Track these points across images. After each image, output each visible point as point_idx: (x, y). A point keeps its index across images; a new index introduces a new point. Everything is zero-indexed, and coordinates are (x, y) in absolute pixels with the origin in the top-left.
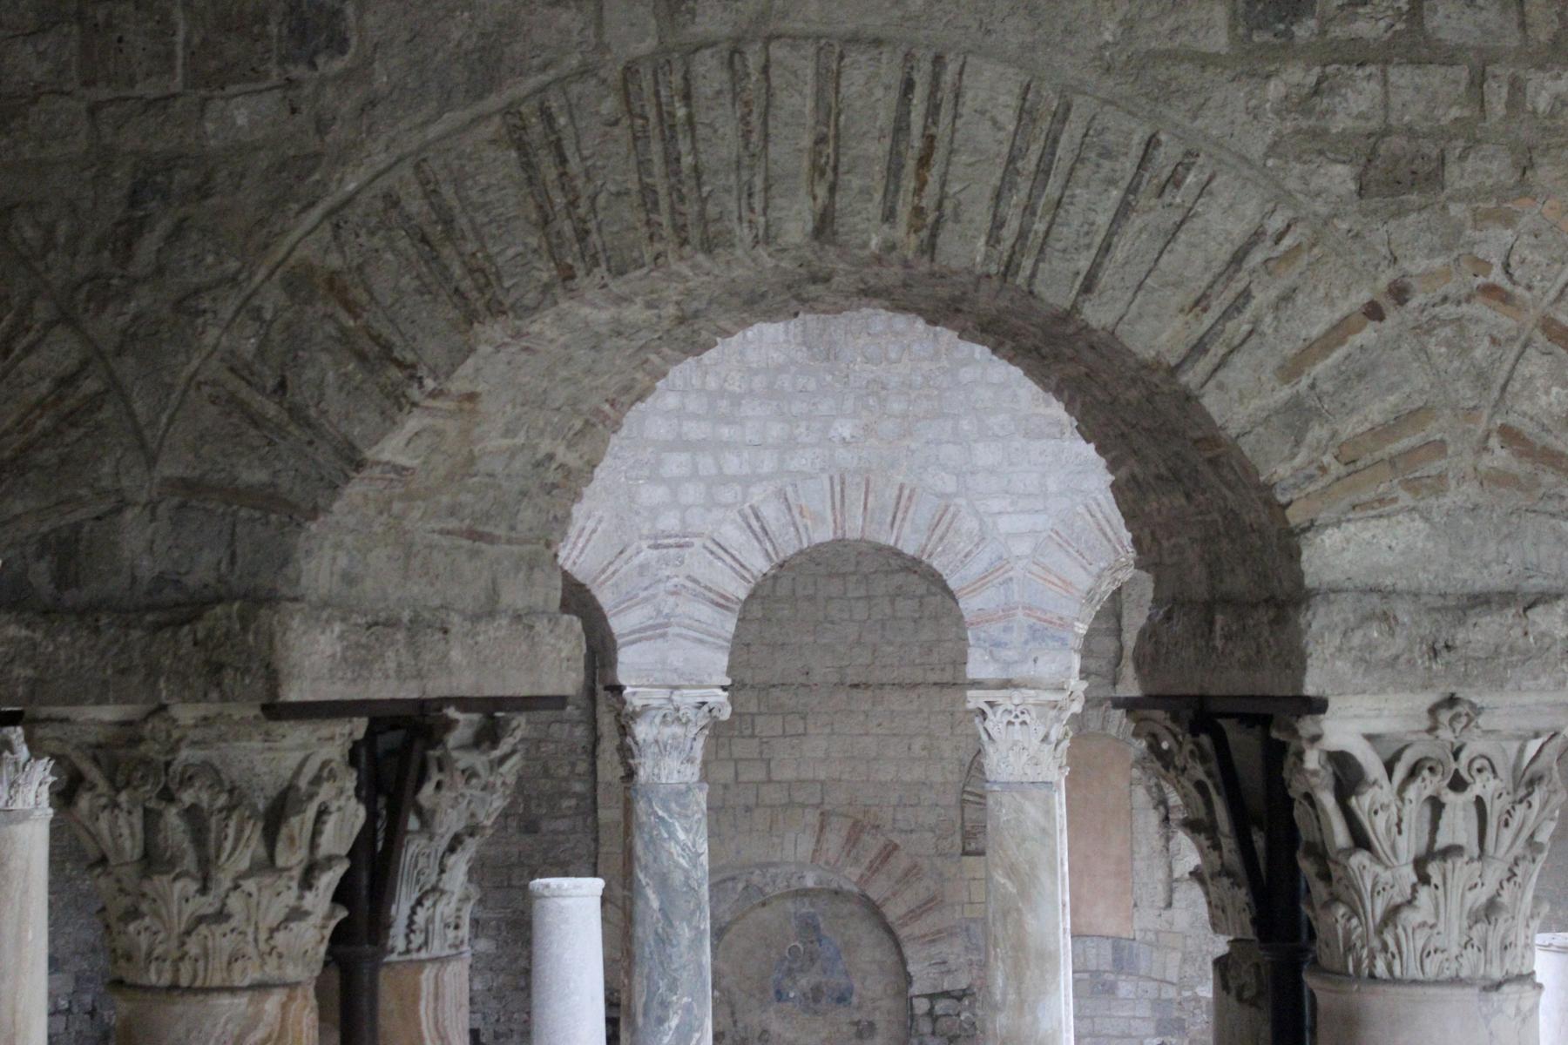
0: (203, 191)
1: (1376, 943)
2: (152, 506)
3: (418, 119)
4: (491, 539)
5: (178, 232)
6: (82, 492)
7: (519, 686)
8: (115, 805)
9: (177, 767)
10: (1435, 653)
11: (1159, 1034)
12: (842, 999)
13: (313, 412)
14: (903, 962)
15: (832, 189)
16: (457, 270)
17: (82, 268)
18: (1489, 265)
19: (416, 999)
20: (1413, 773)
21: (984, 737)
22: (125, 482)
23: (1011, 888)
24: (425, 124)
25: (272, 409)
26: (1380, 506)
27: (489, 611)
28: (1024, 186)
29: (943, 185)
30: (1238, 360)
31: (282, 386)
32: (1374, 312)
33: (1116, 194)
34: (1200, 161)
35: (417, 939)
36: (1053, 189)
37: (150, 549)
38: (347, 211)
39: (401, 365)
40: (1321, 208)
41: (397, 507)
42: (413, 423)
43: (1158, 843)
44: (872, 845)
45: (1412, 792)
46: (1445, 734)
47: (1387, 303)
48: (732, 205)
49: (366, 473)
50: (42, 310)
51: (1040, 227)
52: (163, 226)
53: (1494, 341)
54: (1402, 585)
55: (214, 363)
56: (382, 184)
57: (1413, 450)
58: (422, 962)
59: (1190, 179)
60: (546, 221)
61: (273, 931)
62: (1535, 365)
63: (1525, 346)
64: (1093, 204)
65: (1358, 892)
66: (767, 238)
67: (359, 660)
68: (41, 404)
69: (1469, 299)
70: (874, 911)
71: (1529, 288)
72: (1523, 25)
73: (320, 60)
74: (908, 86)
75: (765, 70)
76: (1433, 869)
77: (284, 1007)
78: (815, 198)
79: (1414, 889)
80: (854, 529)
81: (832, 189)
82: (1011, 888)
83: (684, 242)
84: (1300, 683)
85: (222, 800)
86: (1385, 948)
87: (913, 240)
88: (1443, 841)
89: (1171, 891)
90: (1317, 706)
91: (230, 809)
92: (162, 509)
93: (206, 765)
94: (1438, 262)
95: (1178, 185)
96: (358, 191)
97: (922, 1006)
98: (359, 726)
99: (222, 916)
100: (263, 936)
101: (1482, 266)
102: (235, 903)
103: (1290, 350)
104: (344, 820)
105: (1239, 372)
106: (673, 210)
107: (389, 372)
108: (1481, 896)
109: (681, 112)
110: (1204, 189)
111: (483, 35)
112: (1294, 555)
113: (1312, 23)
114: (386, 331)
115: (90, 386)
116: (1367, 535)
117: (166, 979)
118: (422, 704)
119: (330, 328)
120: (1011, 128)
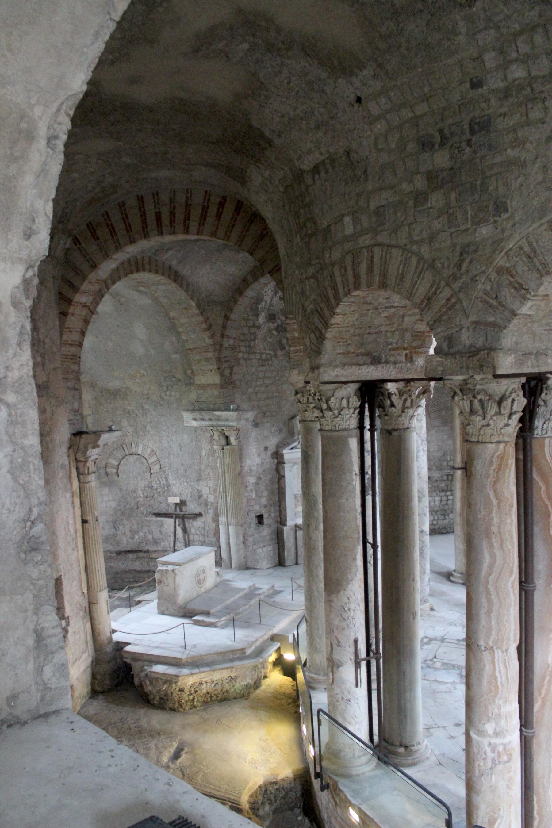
0: (476, 251)
2: (468, 328)
3: (526, 227)
5: (471, 262)
9: (476, 390)
13: (504, 303)
17: (451, 272)
19: (544, 446)
22: (462, 323)
24: (528, 228)
25: (494, 303)
31: (497, 297)
35: (544, 432)
37: (468, 339)
38: (510, 252)
39: (525, 289)
41: (529, 325)
42: (529, 304)
49: (517, 317)
52: (467, 261)
55: (481, 292)
56: (519, 244)
58: (545, 437)
61: (501, 429)
67: (520, 363)
68: (443, 306)
73: (502, 215)
77: (505, 447)
85: (487, 398)
91: (489, 400)
92: (471, 329)
93: (484, 390)
98: (523, 380)
99: (488, 425)
100: (499, 430)
102: (491, 422)
104: (521, 402)
107: (522, 291)
111: (542, 203)
114: (521, 281)
115: (454, 300)
117: (476, 440)
118: (540, 374)
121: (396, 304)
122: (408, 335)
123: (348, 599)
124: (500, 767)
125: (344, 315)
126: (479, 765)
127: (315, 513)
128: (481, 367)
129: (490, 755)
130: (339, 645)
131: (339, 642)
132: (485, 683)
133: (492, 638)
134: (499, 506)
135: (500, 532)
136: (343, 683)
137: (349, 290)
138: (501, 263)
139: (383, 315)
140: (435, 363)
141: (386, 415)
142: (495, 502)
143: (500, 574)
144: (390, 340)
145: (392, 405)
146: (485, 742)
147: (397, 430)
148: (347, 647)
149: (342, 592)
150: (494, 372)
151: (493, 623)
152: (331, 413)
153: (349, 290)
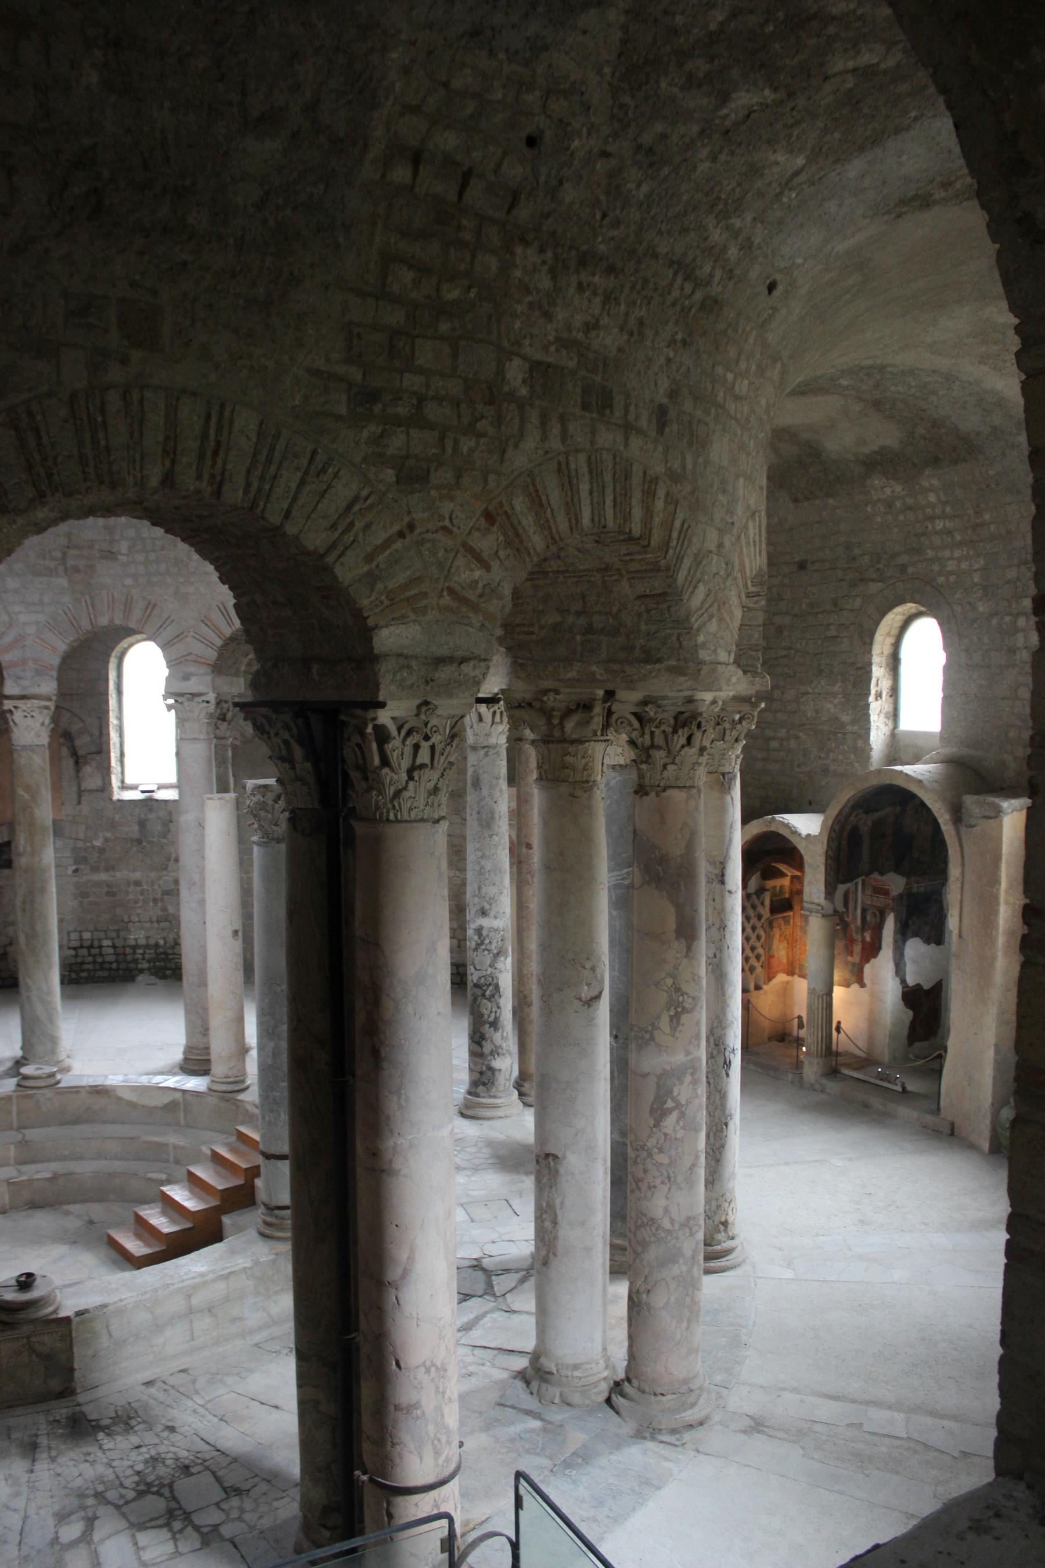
1: (390, 806)
10: (427, 682)
11: (75, 864)
15: (173, 462)
18: (444, 518)
21: (11, 723)
23: (27, 797)
26: (402, 619)
29: (225, 464)
30: (349, 553)
32: (401, 535)
33: (299, 474)
34: (335, 463)
36: (273, 469)
40: (383, 489)
43: (73, 773)
45: (408, 742)
46: (423, 717)
51: (267, 487)
53: (446, 550)
54: (410, 653)
57: (416, 595)
59: (330, 470)
62: (460, 561)
63: (457, 553)
65: (383, 785)
69: (436, 531)
71: (459, 528)
72: (459, 417)
74: (208, 417)
75: (141, 402)
76: (416, 774)
78: (164, 465)
79: (407, 783)
81: (173, 462)
82: (27, 797)
83: (102, 483)
84: (378, 697)
86: (394, 807)
87: (209, 489)
88: (419, 761)
89: (80, 796)
90: (382, 705)
94: (426, 515)
95: (325, 473)
101: (442, 518)
103: (369, 549)
108: (432, 784)
109: (100, 419)
110: (336, 475)
113: (380, 406)
116: (398, 631)
120: (255, 440)
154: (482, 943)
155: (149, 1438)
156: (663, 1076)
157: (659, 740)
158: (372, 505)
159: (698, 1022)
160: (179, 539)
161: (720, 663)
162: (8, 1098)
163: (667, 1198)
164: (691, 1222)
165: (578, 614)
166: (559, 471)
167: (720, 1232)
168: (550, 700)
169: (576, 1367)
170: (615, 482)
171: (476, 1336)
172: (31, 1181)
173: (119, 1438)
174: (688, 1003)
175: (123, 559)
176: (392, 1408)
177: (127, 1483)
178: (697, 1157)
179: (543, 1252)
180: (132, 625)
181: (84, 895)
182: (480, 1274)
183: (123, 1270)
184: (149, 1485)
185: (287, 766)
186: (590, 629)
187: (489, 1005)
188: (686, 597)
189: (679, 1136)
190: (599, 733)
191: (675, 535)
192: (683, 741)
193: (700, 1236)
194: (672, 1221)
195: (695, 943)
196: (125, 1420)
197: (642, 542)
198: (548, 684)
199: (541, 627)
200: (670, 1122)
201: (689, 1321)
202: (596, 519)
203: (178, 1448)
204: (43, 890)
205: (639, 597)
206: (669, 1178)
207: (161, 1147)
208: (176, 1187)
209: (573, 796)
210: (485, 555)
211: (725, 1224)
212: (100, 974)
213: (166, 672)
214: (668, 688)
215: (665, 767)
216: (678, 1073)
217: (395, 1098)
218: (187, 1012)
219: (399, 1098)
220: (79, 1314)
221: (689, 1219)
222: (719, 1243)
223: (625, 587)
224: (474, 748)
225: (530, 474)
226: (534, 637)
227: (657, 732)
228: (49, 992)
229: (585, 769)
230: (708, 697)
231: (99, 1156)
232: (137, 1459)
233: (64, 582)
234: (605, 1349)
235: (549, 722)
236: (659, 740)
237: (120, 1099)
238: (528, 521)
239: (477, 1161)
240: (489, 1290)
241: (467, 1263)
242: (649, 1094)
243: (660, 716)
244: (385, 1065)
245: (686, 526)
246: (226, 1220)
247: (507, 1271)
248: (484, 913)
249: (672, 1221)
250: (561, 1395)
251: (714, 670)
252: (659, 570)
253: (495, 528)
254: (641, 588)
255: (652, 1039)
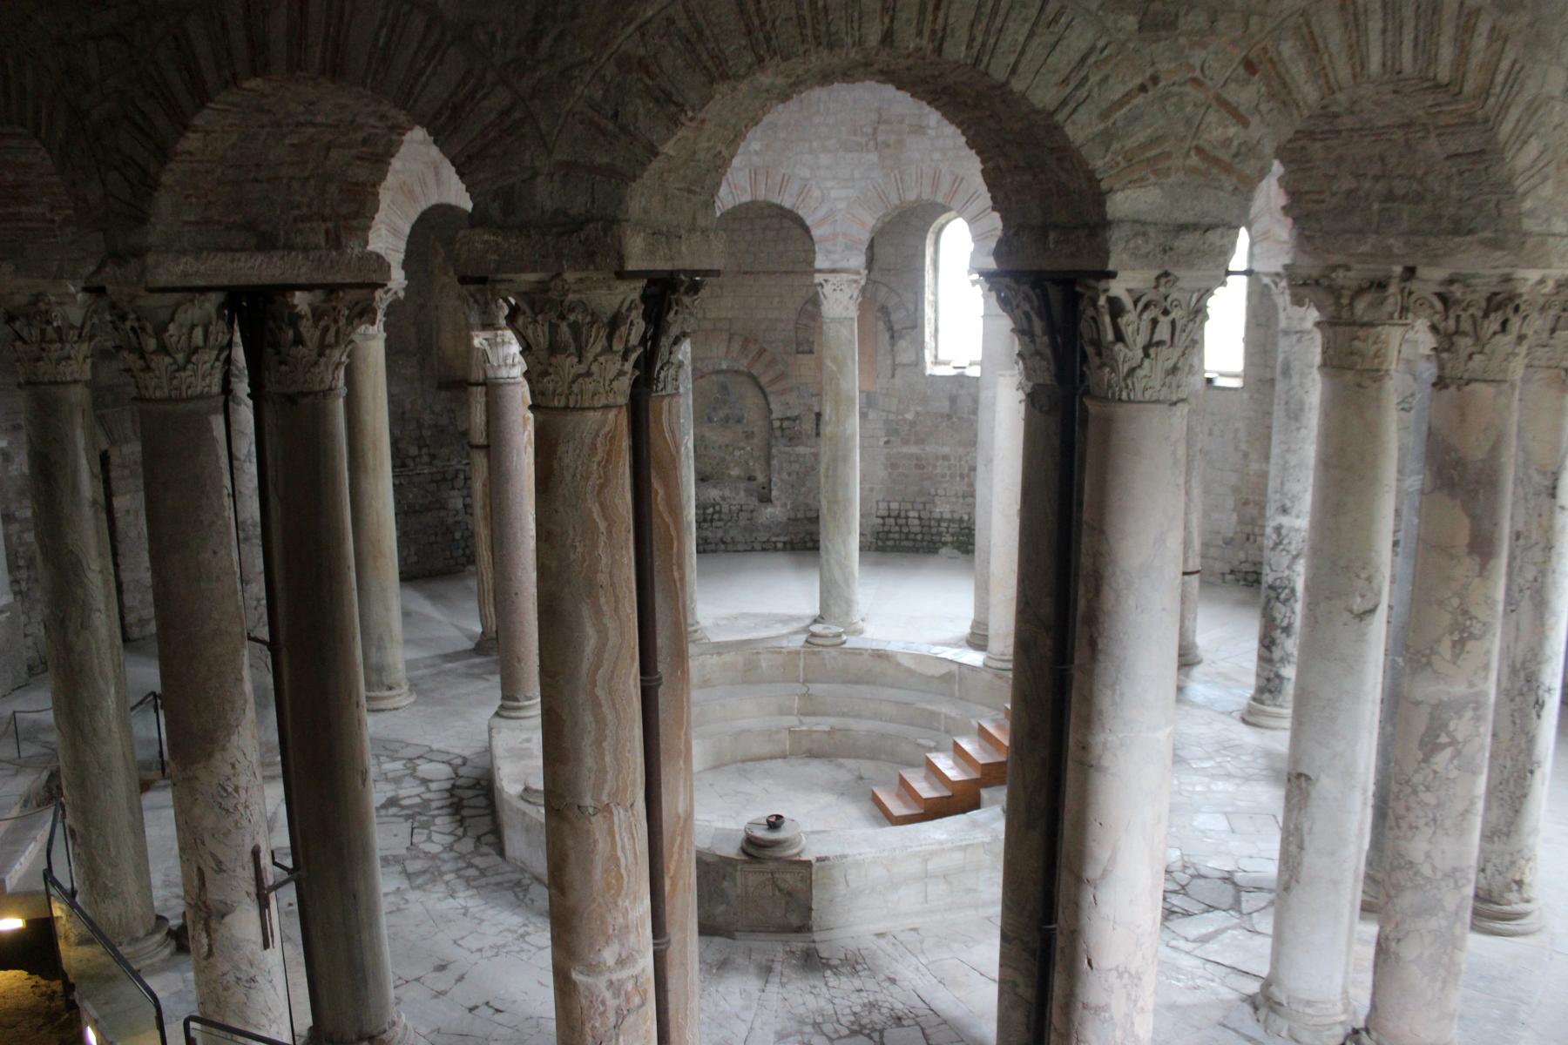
4: (694, 193)
6: (515, 168)
7: (705, 266)
8: (535, 321)
9: (566, 303)
10: (1165, 251)
12: (739, 421)
14: (768, 404)
15: (892, 20)
16: (705, 57)
20: (1146, 307)
22: (537, 164)
25: (611, 126)
26: (1141, 182)
27: (692, 229)
28: (985, 21)
30: (1082, 110)
32: (1143, 88)
33: (1028, 26)
36: (998, 23)
39: (676, 104)
40: (1122, 37)
44: (754, 349)
45: (1145, 316)
46: (1162, 289)
47: (1149, 84)
48: (843, 25)
50: (490, 77)
51: (992, 41)
54: (1149, 219)
59: (1063, 19)
60: (749, 33)
62: (1212, 117)
64: (1017, 31)
66: (860, 43)
69: (1185, 83)
70: (755, 380)
76: (1152, 351)
80: (761, 195)
81: (892, 20)
83: (819, 44)
85: (588, 319)
88: (1156, 338)
89: (894, 370)
90: (1112, 275)
91: (593, 323)
92: (556, 177)
94: (1173, 65)
96: (653, 16)
97: (777, 424)
98: (642, 283)
99: (589, 374)
101: (1191, 68)
102: (595, 368)
103: (1104, 105)
105: (1082, 116)
106: (814, 29)
107: (671, 107)
108: (1170, 364)
112: (1101, 204)
115: (517, 115)
117: (563, 404)
118: (672, 272)
119: (640, 86)
121: (320, 119)
122: (333, 189)
123: (233, 766)
124: (631, 1019)
125: (207, 133)
126: (593, 1028)
127: (79, 591)
128: (591, 255)
129: (612, 1003)
130: (220, 868)
131: (219, 863)
132: (598, 874)
133: (607, 787)
134: (610, 533)
135: (612, 584)
136: (237, 948)
137: (234, 76)
138: (623, 48)
139: (287, 141)
140: (479, 246)
141: (284, 362)
142: (602, 526)
143: (615, 663)
144: (298, 198)
145: (299, 340)
146: (600, 983)
147: (310, 393)
148: (239, 870)
149: (218, 756)
150: (622, 265)
151: (608, 759)
152: (167, 360)
153: (234, 76)
154: (1280, 543)
155: (871, 985)
156: (1438, 706)
157: (1466, 325)
158: (1110, 56)
159: (1488, 652)
160: (924, 103)
161: (1553, 235)
162: (798, 653)
163: (1430, 842)
164: (1458, 875)
165: (1377, 179)
166: (1343, 8)
167: (1511, 890)
168: (1340, 277)
169: (1309, 1004)
170: (1417, 17)
171: (1212, 950)
172: (810, 732)
173: (844, 979)
174: (1477, 628)
175: (932, 133)
176: (1080, 1006)
177: (843, 1020)
178: (1472, 803)
179: (1286, 877)
180: (940, 199)
181: (894, 466)
182: (1230, 887)
183: (882, 826)
184: (863, 1027)
185: (1027, 339)
186: (1390, 196)
187: (1283, 609)
188: (1510, 155)
189: (1452, 776)
190: (1396, 315)
191: (1500, 78)
192: (1496, 326)
193: (1469, 891)
194: (1434, 868)
195: (1492, 563)
196: (853, 964)
197: (1451, 90)
198: (1337, 259)
199: (1334, 194)
200: (1442, 759)
201: (1445, 982)
202: (1389, 63)
203: (895, 999)
204: (846, 459)
205: (1449, 157)
206: (1435, 820)
207: (933, 714)
208: (941, 756)
209: (1359, 385)
210: (1242, 109)
211: (1520, 883)
212: (905, 543)
213: (971, 246)
214: (1480, 266)
215: (1470, 357)
216: (1458, 706)
217: (1109, 693)
218: (977, 588)
219: (1114, 692)
220: (819, 860)
221: (1455, 870)
222: (1509, 903)
223: (1432, 145)
224: (1286, 333)
225: (1304, 13)
226: (1323, 206)
227: (1464, 316)
228: (847, 556)
229: (1376, 355)
230: (1533, 275)
231: (876, 716)
232: (857, 1002)
233: (873, 157)
234: (1345, 991)
235: (1338, 303)
236: (1466, 325)
237: (899, 664)
238: (1298, 71)
239: (1251, 771)
240: (1236, 905)
241: (1219, 874)
242: (1420, 725)
243: (1469, 297)
244: (1101, 657)
245: (1517, 67)
246: (985, 793)
247: (1260, 889)
248: (1284, 510)
249: (1434, 868)
250: (1289, 1029)
251: (1543, 243)
252: (1474, 124)
253: (1257, 77)
254: (1454, 146)
255: (1429, 664)
